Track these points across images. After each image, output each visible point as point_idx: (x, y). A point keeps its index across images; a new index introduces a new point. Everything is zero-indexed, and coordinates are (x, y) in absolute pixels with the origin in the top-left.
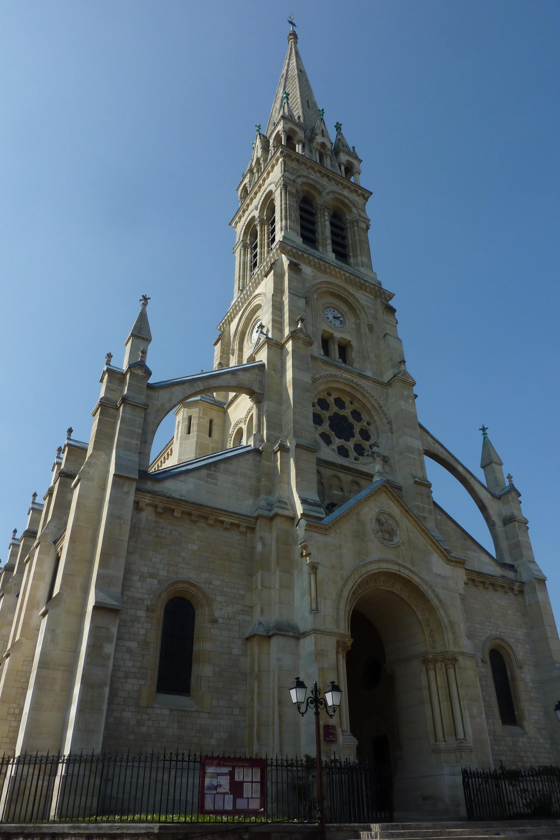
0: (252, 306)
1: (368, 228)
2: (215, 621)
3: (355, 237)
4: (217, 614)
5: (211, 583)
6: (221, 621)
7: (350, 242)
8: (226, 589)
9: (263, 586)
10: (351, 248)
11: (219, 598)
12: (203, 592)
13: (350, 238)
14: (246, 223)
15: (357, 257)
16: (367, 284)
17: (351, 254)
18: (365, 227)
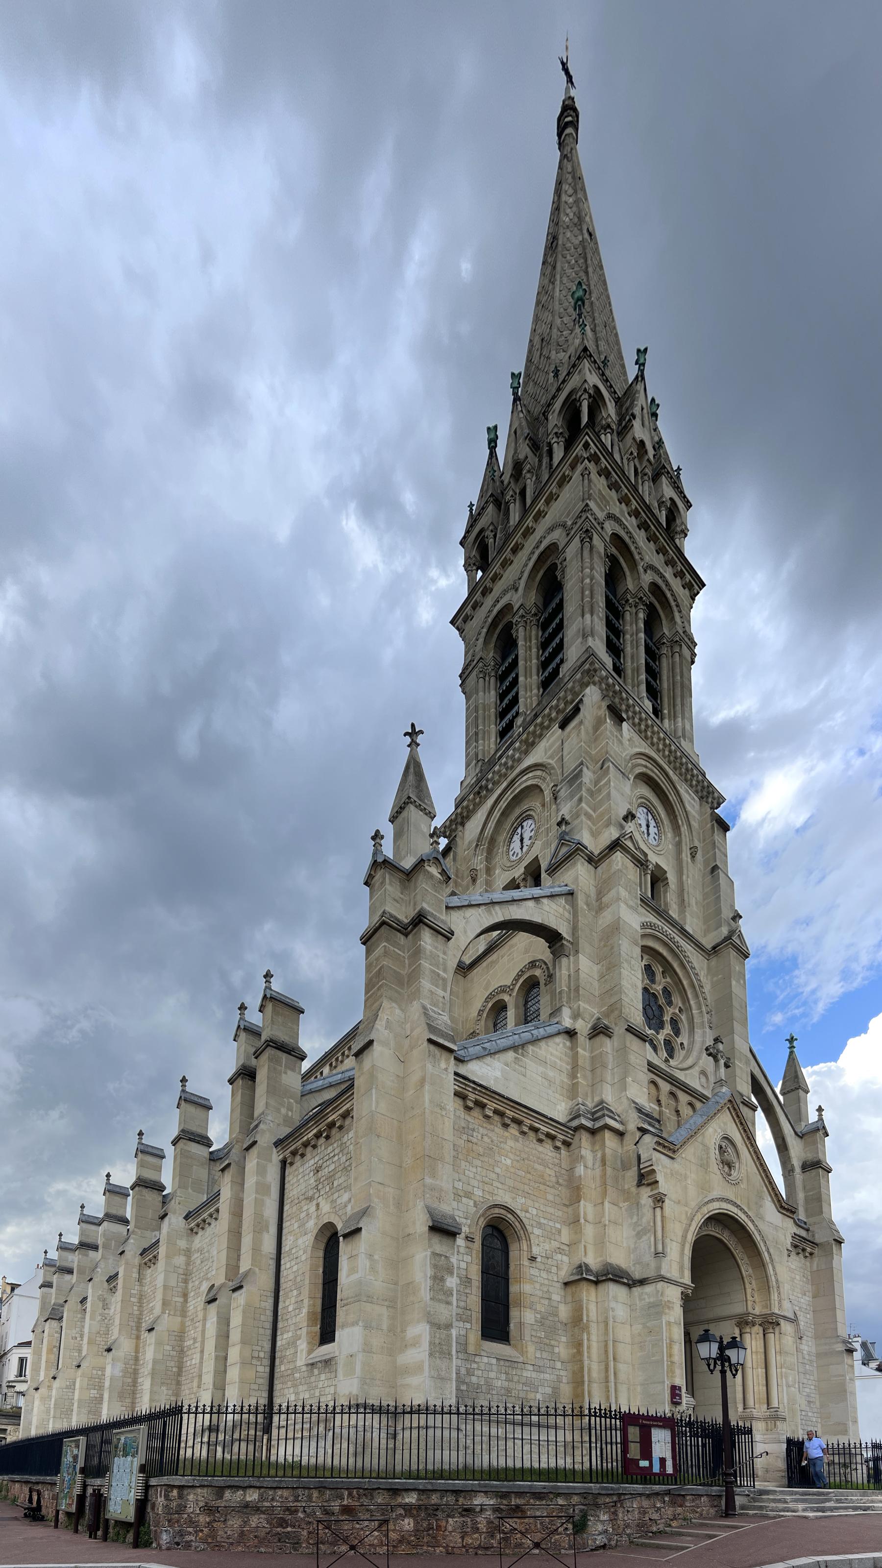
0: (516, 789)
1: (693, 662)
2: (533, 1259)
3: (673, 677)
4: (536, 1250)
5: (527, 1211)
6: (539, 1259)
7: (665, 685)
8: (542, 1221)
9: (586, 1220)
10: (666, 700)
11: (537, 1231)
12: (521, 1221)
13: (665, 678)
14: (490, 620)
15: (675, 717)
16: (695, 772)
17: (666, 711)
18: (690, 660)
